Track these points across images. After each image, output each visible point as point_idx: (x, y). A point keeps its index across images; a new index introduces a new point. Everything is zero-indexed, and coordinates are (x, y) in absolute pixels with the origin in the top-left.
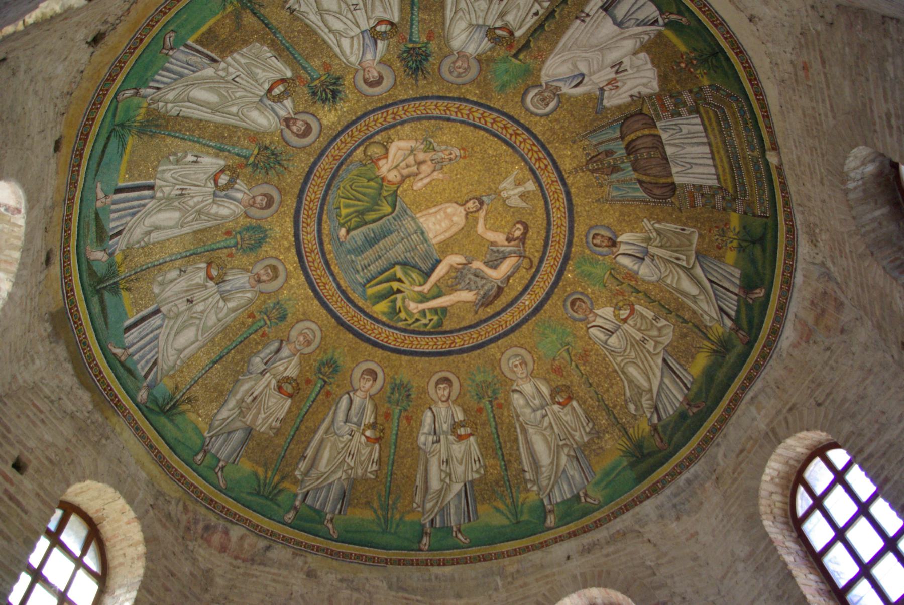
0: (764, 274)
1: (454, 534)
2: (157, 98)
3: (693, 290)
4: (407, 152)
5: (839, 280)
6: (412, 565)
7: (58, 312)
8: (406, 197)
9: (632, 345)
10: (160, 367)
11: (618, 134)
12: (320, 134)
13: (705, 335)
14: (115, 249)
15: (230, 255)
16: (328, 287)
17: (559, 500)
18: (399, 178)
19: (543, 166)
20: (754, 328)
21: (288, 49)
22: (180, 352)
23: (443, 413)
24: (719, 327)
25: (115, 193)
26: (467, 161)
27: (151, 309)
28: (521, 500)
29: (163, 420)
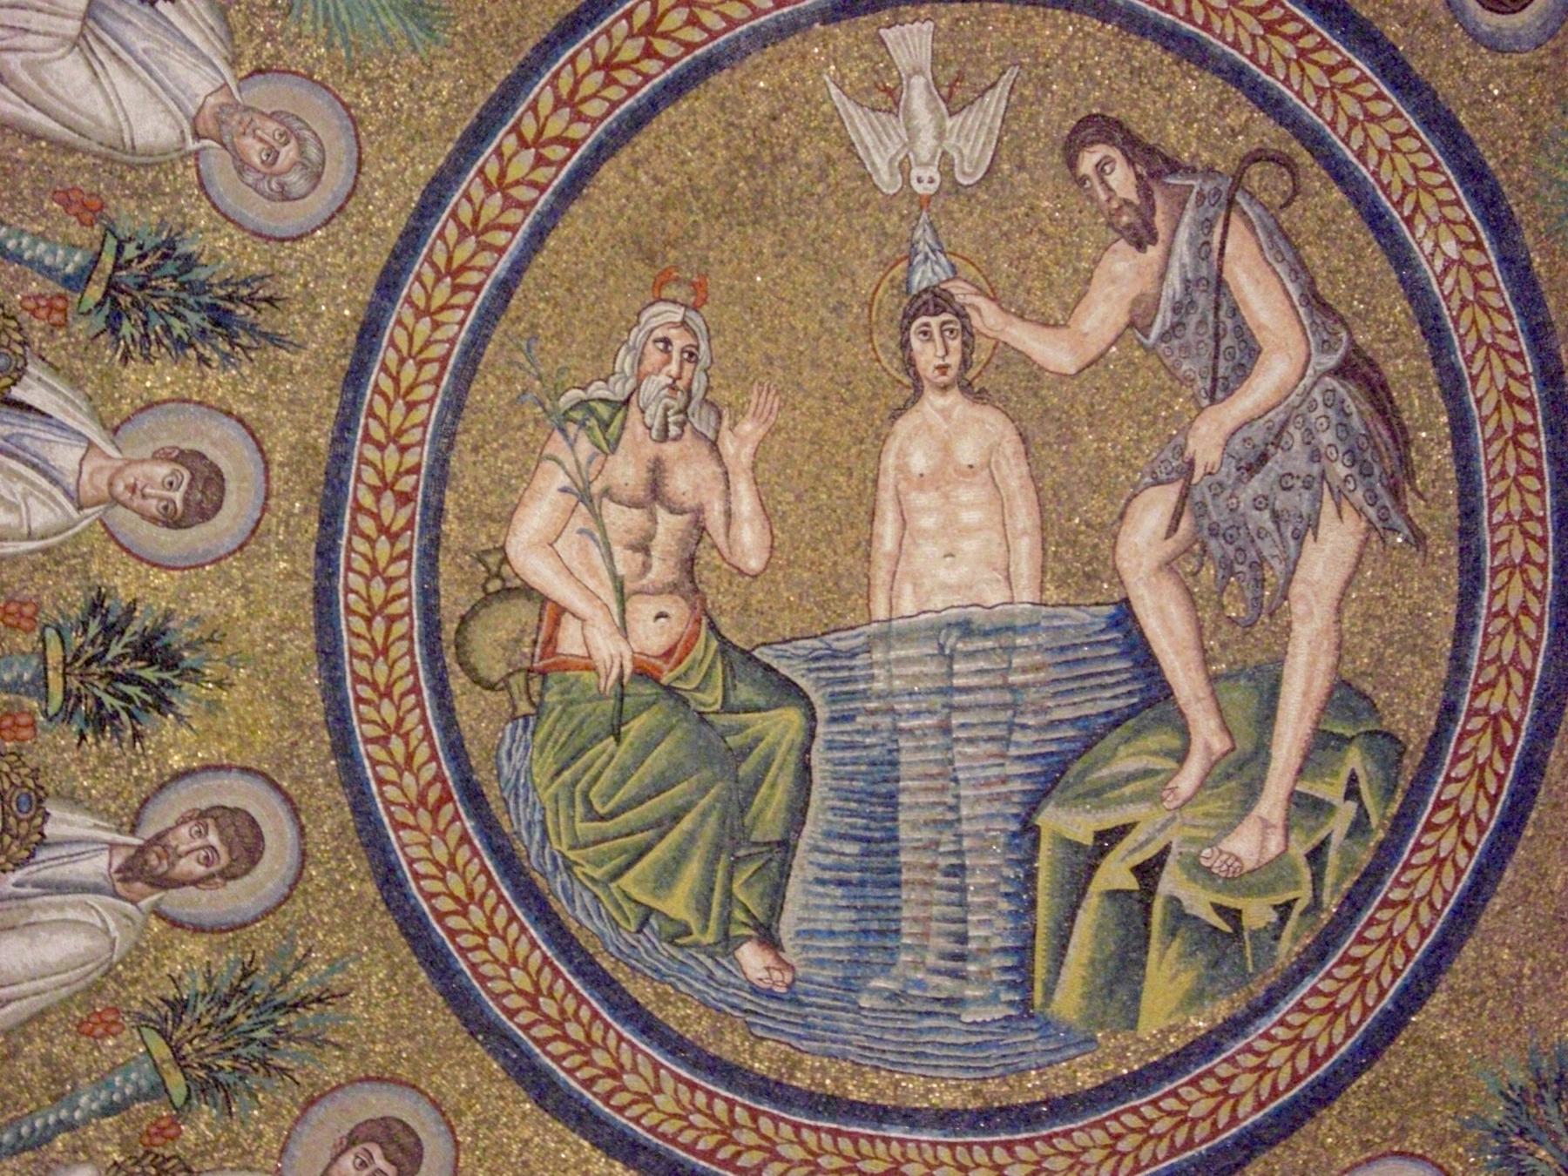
4: (581, 518)
12: (287, 798)
18: (677, 608)
26: (720, 281)
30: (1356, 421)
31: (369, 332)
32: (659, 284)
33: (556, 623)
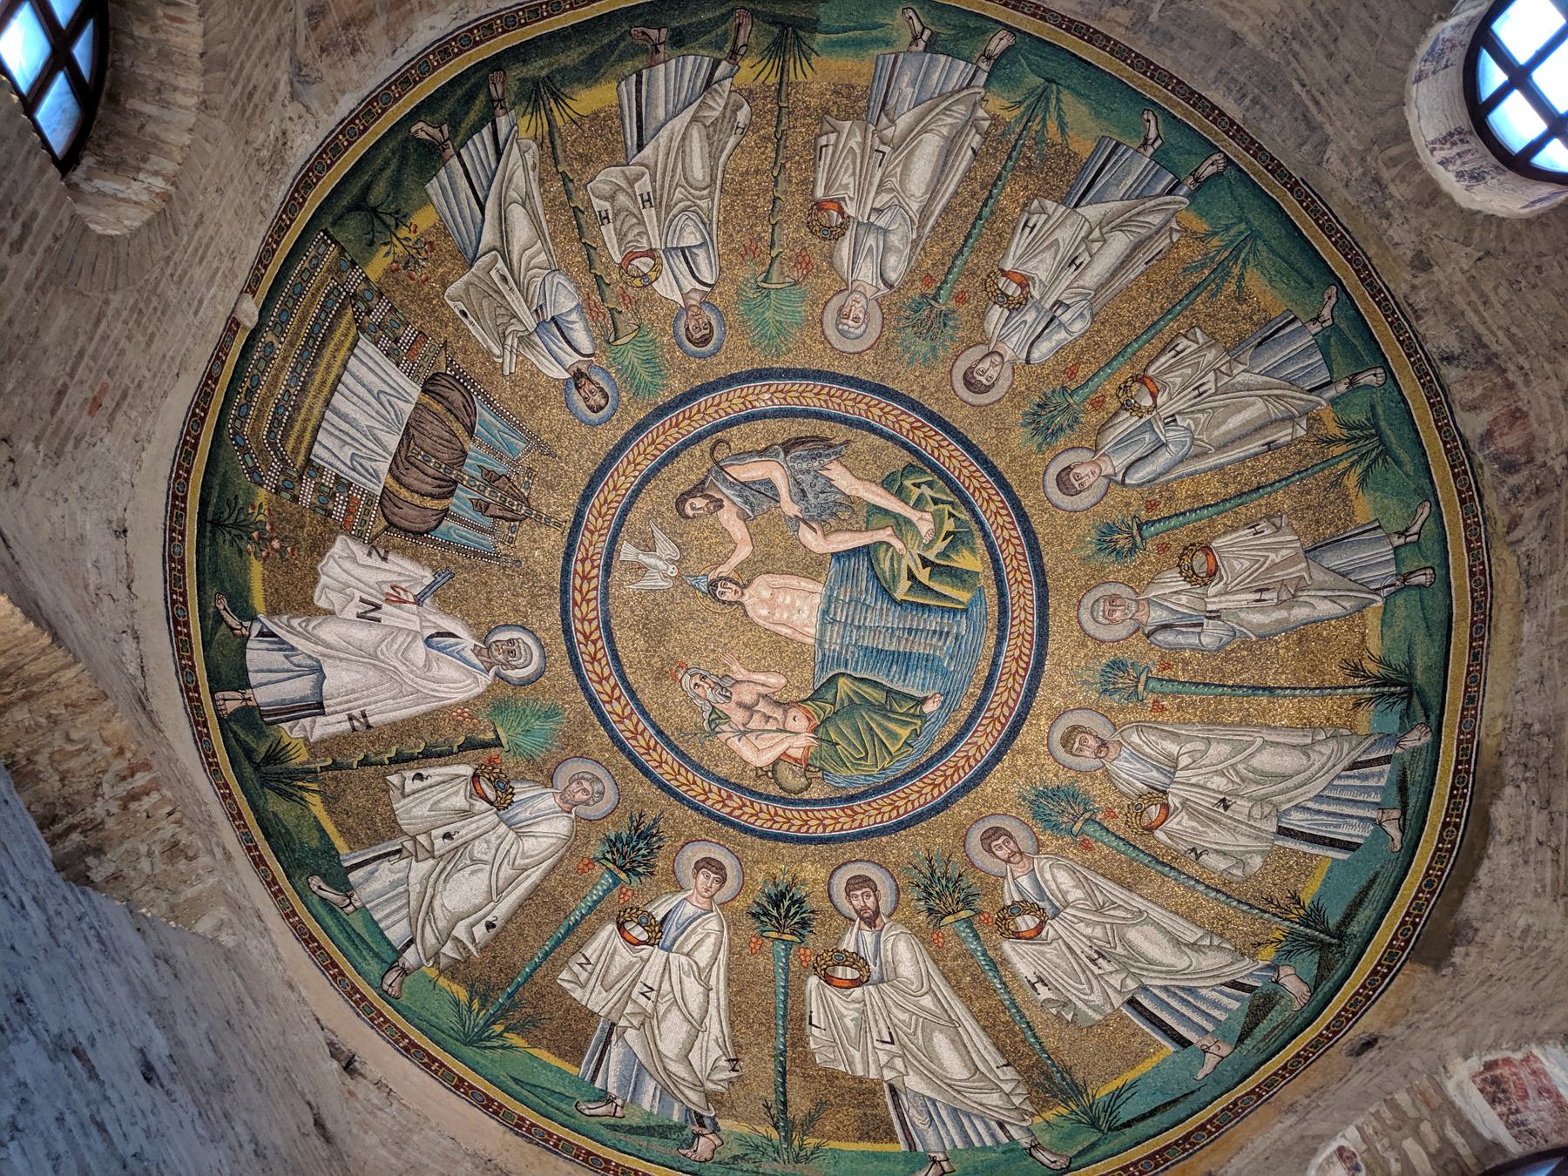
0: (394, 153)
1: (1159, 142)
2: (1013, 1114)
3: (517, 214)
4: (752, 737)
5: (287, 53)
6: (1261, 148)
7: (1424, 962)
8: (807, 678)
9: (669, 208)
10: (1354, 754)
11: (447, 523)
12: (844, 864)
13: (550, 133)
14: (1261, 969)
15: (1110, 813)
16: (1017, 653)
17: (963, 63)
18: (793, 712)
19: (588, 565)
20: (469, 87)
21: (784, 1016)
22: (1304, 749)
23: (1015, 339)
24: (523, 130)
25: (1190, 1043)
27: (1290, 844)
28: (1017, 112)
29: (1420, 678)
30: (803, 453)
31: (663, 787)
32: (675, 678)
33: (789, 757)
